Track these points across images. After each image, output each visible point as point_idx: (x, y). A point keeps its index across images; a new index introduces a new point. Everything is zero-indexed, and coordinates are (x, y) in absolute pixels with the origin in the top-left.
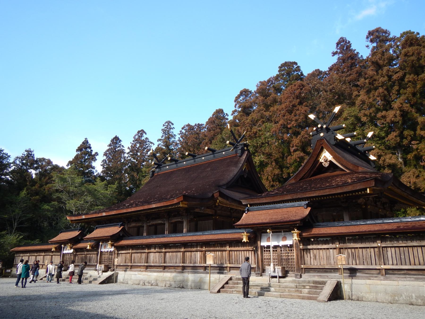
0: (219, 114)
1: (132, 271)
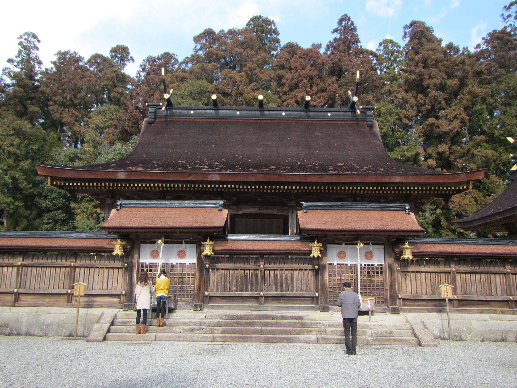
0: (122, 53)
1: (460, 311)
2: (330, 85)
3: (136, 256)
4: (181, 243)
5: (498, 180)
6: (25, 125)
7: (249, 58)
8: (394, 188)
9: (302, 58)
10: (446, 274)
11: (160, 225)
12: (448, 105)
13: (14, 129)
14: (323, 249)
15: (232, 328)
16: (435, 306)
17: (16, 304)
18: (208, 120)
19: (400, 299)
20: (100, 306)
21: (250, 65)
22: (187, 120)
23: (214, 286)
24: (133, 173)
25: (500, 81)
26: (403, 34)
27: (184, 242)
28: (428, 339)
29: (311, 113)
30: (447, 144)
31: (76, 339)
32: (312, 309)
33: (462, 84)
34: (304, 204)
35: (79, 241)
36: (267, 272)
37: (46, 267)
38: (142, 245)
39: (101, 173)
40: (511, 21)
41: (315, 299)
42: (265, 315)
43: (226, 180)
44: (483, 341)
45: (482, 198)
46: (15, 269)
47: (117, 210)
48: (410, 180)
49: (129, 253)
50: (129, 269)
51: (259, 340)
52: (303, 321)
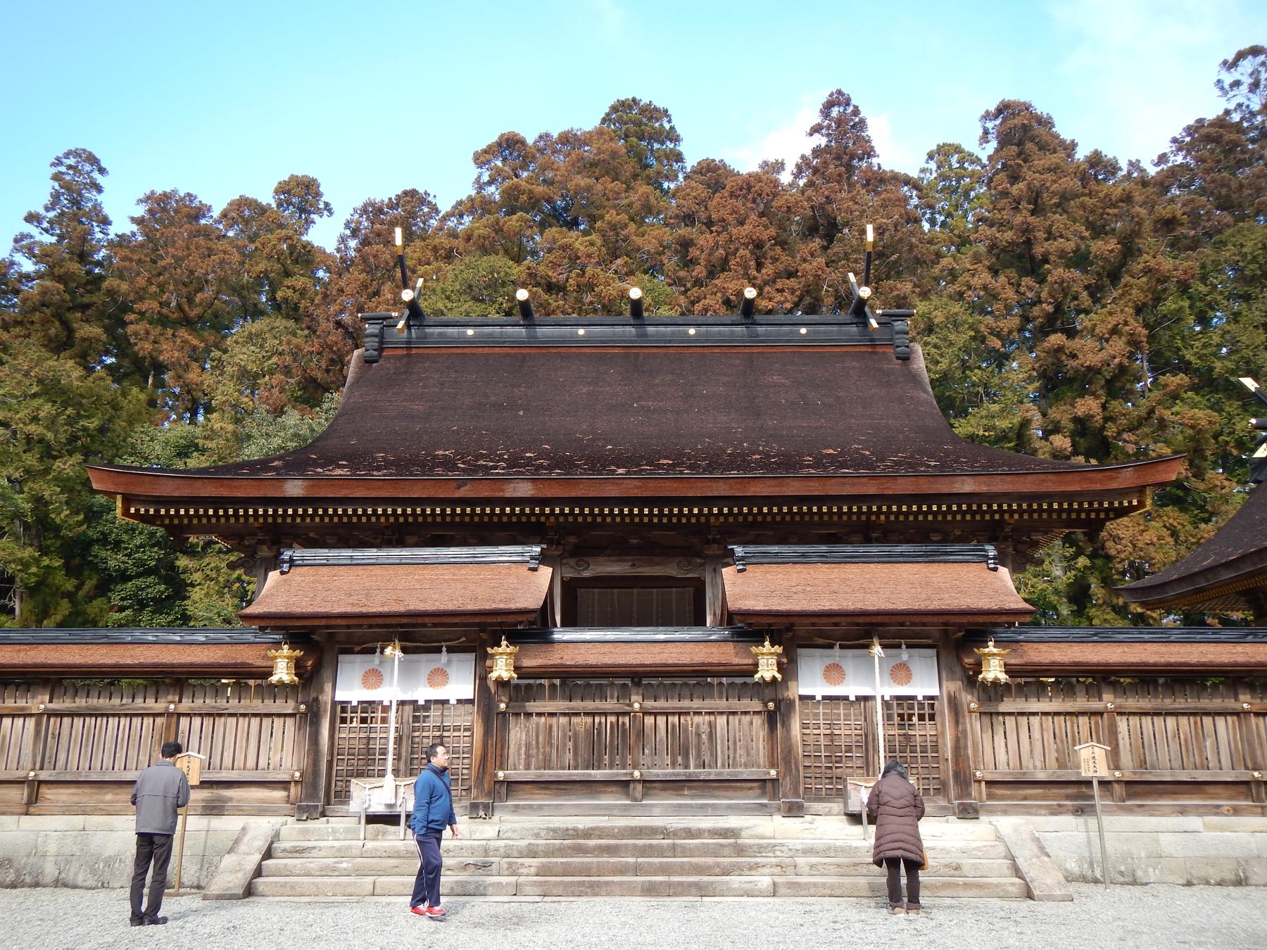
0: (302, 196)
1: (1130, 810)
2: (805, 260)
3: (328, 687)
4: (438, 650)
5: (1226, 483)
6: (68, 370)
7: (608, 200)
8: (959, 506)
9: (737, 197)
10: (1093, 718)
11: (386, 609)
12: (1096, 301)
13: (40, 381)
14: (785, 660)
15: (564, 860)
16: (1068, 797)
17: (32, 810)
18: (509, 351)
19: (980, 782)
20: (240, 811)
21: (611, 216)
22: (458, 351)
23: (519, 755)
24: (324, 483)
25: (1221, 242)
26: (981, 132)
27: (444, 649)
28: (1049, 881)
29: (760, 329)
30: (1097, 397)
31: (178, 895)
32: (762, 810)
33: (1129, 250)
34: (739, 550)
35: (189, 649)
36: (649, 720)
37: (108, 716)
38: (341, 657)
39: (245, 482)
40: (1241, 95)
41: (769, 785)
42: (646, 827)
43: (549, 495)
44: (1189, 884)
45: (1189, 527)
46: (31, 723)
47: (283, 573)
48: (1000, 485)
49: (311, 676)
50: (310, 718)
51: (629, 890)
52: (740, 841)
